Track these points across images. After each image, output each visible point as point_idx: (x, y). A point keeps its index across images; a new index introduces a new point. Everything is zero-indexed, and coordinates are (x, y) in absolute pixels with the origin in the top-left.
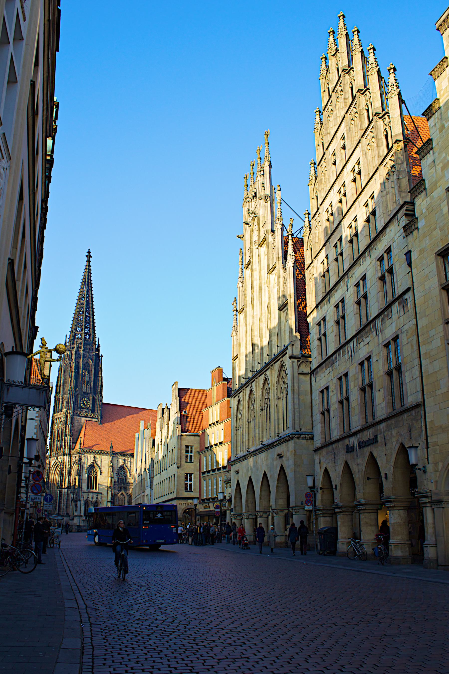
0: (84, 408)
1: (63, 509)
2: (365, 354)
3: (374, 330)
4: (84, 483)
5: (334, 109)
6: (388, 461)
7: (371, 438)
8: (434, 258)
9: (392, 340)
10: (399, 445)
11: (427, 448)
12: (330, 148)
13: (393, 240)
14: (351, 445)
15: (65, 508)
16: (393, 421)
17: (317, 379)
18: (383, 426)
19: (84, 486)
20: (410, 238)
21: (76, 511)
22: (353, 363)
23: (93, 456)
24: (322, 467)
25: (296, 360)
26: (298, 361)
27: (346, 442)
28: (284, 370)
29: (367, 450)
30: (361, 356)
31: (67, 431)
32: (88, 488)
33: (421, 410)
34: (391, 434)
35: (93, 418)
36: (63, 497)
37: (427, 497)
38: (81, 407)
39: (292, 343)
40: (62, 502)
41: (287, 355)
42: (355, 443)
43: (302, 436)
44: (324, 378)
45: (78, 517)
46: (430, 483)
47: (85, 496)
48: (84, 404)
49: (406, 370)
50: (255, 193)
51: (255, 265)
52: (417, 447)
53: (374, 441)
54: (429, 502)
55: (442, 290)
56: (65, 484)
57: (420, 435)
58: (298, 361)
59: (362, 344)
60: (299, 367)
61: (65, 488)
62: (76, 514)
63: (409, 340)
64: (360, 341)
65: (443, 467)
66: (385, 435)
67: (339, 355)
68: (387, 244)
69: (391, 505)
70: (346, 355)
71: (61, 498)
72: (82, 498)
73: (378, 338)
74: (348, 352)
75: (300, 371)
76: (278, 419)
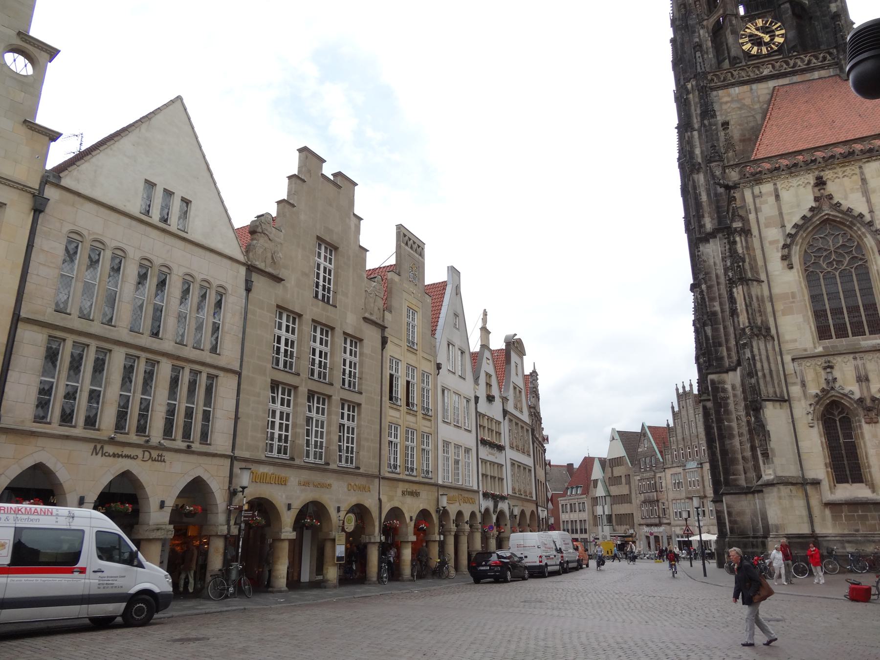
0: (758, 56)
1: (744, 458)
4: (788, 311)
15: (748, 454)
19: (796, 329)
21: (766, 455)
23: (811, 178)
31: (698, 151)
32: (823, 333)
35: (813, 69)
36: (732, 407)
38: (747, 55)
40: (736, 432)
45: (784, 490)
47: (810, 376)
48: (757, 41)
56: (729, 349)
61: (735, 370)
62: (768, 475)
71: (727, 412)
72: (795, 390)
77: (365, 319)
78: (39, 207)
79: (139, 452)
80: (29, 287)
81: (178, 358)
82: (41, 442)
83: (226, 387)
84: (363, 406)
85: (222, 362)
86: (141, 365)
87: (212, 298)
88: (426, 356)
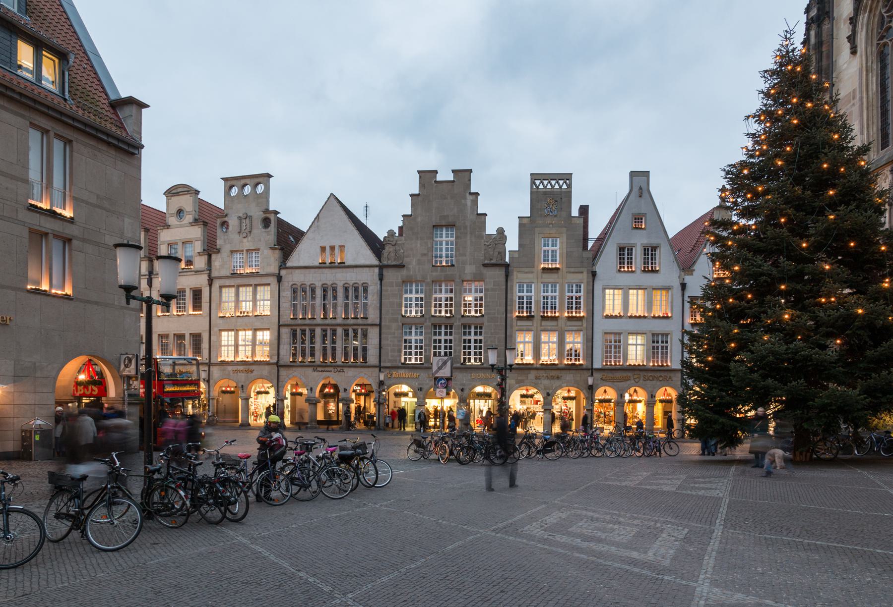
77: (485, 265)
78: (280, 279)
79: (332, 369)
80: (281, 313)
81: (345, 325)
82: (294, 369)
83: (373, 333)
84: (486, 324)
85: (369, 321)
86: (329, 331)
87: (361, 289)
88: (572, 270)
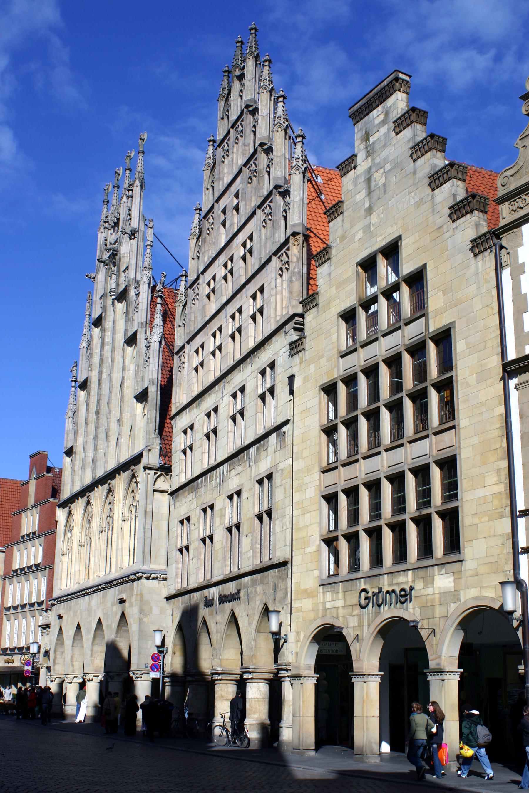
2: (235, 486)
3: (248, 459)
5: (230, 151)
6: (250, 623)
7: (234, 592)
8: (318, 391)
9: (266, 476)
10: (263, 605)
11: (291, 613)
12: (221, 202)
13: (277, 353)
14: (211, 598)
16: (258, 576)
17: (177, 504)
18: (247, 579)
20: (297, 358)
22: (221, 493)
24: (174, 621)
25: (152, 472)
26: (155, 473)
27: (205, 592)
28: (135, 482)
29: (228, 606)
30: (231, 488)
33: (288, 569)
34: (256, 591)
37: (287, 670)
39: (149, 448)
41: (141, 466)
42: (215, 596)
43: (153, 576)
44: (186, 505)
46: (290, 654)
49: (276, 518)
50: (118, 220)
51: (108, 324)
52: (280, 611)
53: (235, 597)
54: (288, 677)
55: (322, 432)
57: (285, 597)
58: (155, 473)
59: (233, 472)
60: (155, 481)
63: (284, 482)
64: (231, 468)
65: (305, 636)
66: (249, 591)
67: (205, 479)
68: (271, 356)
69: (250, 677)
70: (214, 482)
73: (251, 470)
74: (216, 479)
75: (157, 487)
76: (122, 549)
